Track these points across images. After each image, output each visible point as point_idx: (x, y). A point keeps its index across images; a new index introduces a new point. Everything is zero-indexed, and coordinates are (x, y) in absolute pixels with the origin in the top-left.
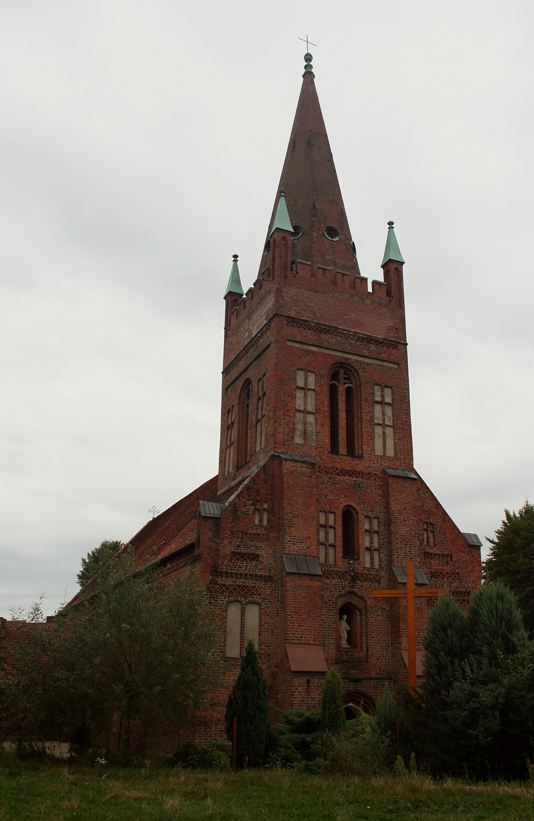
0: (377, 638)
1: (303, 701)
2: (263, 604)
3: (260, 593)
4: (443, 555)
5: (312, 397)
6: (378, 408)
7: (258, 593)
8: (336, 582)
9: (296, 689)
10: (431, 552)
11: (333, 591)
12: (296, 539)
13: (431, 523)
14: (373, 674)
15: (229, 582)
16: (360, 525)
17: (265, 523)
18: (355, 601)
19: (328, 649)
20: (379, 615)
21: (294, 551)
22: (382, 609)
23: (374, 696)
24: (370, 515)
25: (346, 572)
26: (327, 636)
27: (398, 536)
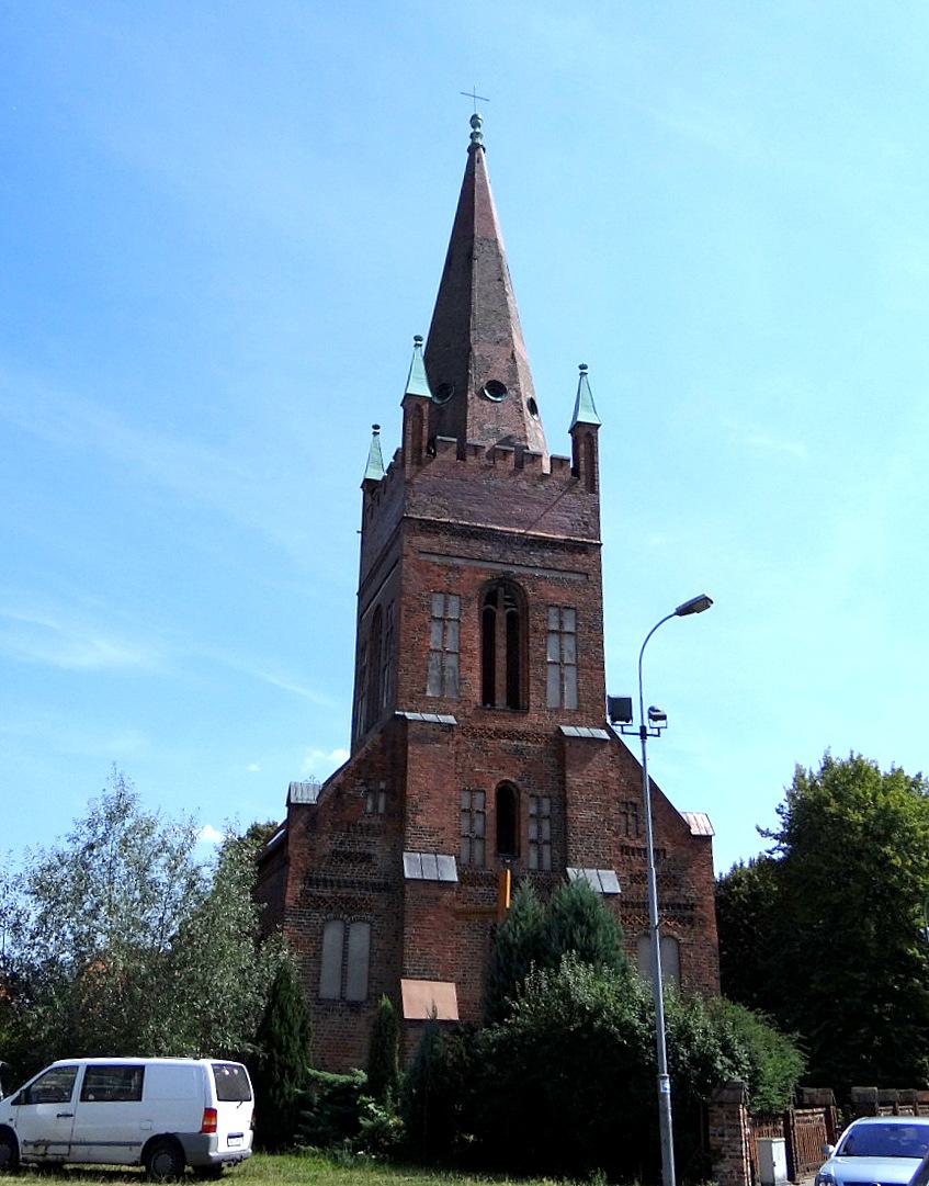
5: (454, 630)
6: (553, 640)
10: (632, 845)
13: (631, 803)
15: (327, 893)
16: (522, 810)
17: (381, 809)
24: (538, 793)
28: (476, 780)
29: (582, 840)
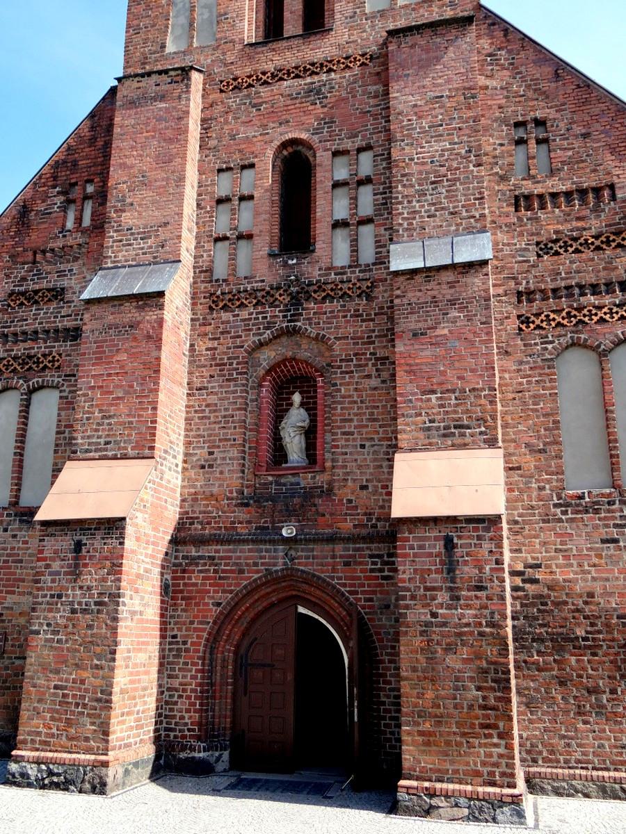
1: (60, 596)
2: (64, 388)
3: (59, 367)
4: (583, 192)
7: (57, 364)
8: (252, 314)
9: (48, 566)
10: (538, 190)
11: (240, 336)
12: (132, 234)
14: (347, 526)
17: (87, 222)
18: (305, 351)
19: (221, 473)
20: (369, 376)
21: (126, 261)
22: (377, 359)
23: (344, 585)
24: (348, 145)
25: (278, 288)
26: (220, 440)
27: (414, 169)
28: (240, 151)
29: (422, 194)
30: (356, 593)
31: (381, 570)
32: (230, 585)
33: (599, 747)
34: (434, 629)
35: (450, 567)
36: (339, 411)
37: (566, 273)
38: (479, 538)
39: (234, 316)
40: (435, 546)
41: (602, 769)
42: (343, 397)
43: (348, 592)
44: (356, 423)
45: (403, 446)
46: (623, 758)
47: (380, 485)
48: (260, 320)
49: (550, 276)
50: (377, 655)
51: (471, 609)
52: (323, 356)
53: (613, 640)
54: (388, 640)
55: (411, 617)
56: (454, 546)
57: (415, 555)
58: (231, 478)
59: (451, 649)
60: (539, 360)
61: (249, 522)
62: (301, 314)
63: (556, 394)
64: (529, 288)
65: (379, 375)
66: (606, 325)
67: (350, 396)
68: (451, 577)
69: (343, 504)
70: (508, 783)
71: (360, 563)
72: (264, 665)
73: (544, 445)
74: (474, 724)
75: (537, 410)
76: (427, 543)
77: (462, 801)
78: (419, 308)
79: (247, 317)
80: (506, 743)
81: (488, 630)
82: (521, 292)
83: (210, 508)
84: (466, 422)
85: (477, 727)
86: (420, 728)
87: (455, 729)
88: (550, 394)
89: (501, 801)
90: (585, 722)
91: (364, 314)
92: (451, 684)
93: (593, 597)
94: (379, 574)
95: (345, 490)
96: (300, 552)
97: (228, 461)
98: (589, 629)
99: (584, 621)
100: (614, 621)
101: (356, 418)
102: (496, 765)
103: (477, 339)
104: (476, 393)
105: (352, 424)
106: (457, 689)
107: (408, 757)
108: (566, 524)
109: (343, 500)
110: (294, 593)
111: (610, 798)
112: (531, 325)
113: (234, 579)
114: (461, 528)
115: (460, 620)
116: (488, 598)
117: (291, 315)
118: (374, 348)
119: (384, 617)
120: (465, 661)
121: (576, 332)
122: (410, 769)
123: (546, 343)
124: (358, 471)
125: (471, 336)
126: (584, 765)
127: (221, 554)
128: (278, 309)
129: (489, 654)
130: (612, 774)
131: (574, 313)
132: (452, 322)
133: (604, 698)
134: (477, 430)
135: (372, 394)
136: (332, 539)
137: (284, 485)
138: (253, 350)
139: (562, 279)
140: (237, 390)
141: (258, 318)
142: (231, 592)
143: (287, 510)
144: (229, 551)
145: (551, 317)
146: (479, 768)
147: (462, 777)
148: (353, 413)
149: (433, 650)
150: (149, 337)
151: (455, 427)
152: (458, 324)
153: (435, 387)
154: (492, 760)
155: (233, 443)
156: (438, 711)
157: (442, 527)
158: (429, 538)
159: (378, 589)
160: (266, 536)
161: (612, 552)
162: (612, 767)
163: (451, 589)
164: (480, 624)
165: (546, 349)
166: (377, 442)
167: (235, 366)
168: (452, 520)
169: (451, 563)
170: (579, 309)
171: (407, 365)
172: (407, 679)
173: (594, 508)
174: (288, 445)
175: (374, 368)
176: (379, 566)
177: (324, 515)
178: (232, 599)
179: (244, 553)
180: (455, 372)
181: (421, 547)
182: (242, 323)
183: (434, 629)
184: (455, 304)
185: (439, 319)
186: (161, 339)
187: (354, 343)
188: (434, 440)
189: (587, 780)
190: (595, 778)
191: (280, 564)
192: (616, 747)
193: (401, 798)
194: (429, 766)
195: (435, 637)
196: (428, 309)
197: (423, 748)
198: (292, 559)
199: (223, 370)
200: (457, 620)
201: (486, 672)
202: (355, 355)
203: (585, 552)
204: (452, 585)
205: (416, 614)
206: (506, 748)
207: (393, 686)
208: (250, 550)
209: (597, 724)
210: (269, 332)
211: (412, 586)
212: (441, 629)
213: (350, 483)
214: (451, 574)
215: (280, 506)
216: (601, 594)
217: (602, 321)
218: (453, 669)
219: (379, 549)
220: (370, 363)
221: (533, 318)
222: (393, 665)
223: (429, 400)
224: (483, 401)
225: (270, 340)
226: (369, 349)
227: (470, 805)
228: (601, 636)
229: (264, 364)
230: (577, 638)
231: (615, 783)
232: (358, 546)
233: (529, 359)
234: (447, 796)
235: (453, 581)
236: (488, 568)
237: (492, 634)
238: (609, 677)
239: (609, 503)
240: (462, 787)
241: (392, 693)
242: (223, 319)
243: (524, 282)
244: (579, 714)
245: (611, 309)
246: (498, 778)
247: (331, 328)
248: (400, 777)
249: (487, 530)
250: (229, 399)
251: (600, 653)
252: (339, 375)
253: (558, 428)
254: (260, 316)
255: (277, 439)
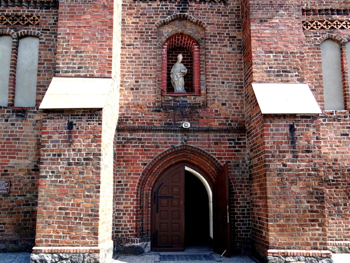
0: (221, 76)
1: (59, 155)
2: (42, 37)
3: (38, 24)
7: (36, 22)
8: (159, 5)
9: (50, 137)
11: (152, 17)
14: (215, 124)
18: (189, 30)
19: (144, 93)
20: (226, 46)
22: (230, 37)
23: (215, 154)
26: (142, 75)
30: (221, 158)
31: (234, 147)
32: (151, 154)
33: (338, 230)
34: (285, 172)
35: (293, 141)
36: (210, 63)
37: (326, 2)
38: (308, 126)
39: (148, 5)
40: (284, 130)
41: (339, 240)
42: (212, 56)
43: (218, 158)
44: (219, 70)
45: (255, 80)
46: (349, 234)
47: (232, 103)
48: (164, 9)
49: (318, 3)
50: (233, 190)
51: (304, 162)
52: (199, 33)
53: (346, 181)
54: (239, 182)
55: (272, 166)
56: (295, 130)
57: (274, 134)
58: (149, 96)
59: (293, 182)
60: (313, 45)
61: (161, 120)
62: (188, 9)
63: (321, 62)
64: (308, 8)
65: (231, 46)
66: (345, 30)
67: (216, 56)
68: (293, 146)
69: (213, 113)
70: (323, 248)
71: (223, 143)
72: (168, 197)
73: (315, 87)
74: (306, 220)
75: (311, 70)
76: (280, 128)
77: (302, 258)
78: (263, 7)
79: (156, 7)
80: (323, 228)
81: (313, 173)
82: (304, 9)
83: (137, 112)
84: (288, 69)
85: (308, 221)
86: (278, 223)
87: (296, 223)
88: (318, 62)
89: (321, 256)
90: (332, 219)
91: (223, 12)
92: (294, 200)
93: (337, 161)
94: (233, 149)
95: (214, 105)
96: (191, 137)
97: (147, 87)
98: (335, 176)
99: (333, 172)
100: (346, 172)
101: (219, 68)
102: (318, 239)
103: (294, 27)
104: (293, 55)
105: (217, 71)
106: (297, 202)
107: (272, 238)
108: (325, 126)
109: (212, 110)
110: (184, 159)
111: (344, 252)
112: (309, 27)
113: (153, 151)
114: (298, 120)
115: (298, 167)
116: (312, 156)
117: (182, 9)
118: (228, 31)
119: (236, 171)
120: (301, 188)
121: (331, 32)
122: (273, 244)
123: (316, 36)
124: (221, 96)
125: (290, 25)
126: (332, 239)
127: (145, 137)
128: (174, 4)
129: (314, 184)
130: (344, 242)
131: (329, 23)
132: (281, 16)
133: (341, 208)
134: (294, 74)
135: (228, 56)
136: (208, 131)
137: (178, 102)
138: (160, 26)
139: (324, 5)
140: (151, 47)
141: (163, 8)
142: (152, 158)
143: (182, 115)
144: (150, 136)
145: (318, 24)
146: (309, 241)
147: (300, 246)
148: (218, 65)
149: (284, 183)
150: (105, 7)
151: (283, 72)
152: (284, 18)
153: (272, 50)
154: (316, 237)
155: (150, 76)
156: (287, 214)
157: (288, 119)
158: (281, 126)
159: (233, 156)
160: (168, 128)
161: (346, 140)
162: (344, 239)
163: (293, 152)
164: (309, 170)
165: (316, 39)
166: (230, 81)
167: (149, 33)
168: (294, 116)
169: (293, 138)
170: (332, 21)
171: (257, 37)
172: (270, 198)
173: (337, 119)
174: (176, 82)
175: (229, 42)
176: (233, 145)
177: (202, 118)
178: (153, 161)
179: (159, 137)
180: (282, 43)
181: (277, 130)
182: (154, 10)
183: (285, 172)
184: (282, 7)
185: (274, 14)
186: (113, 8)
187: (217, 27)
188: (272, 78)
189: (334, 245)
190: (337, 244)
191: (180, 143)
192: (346, 230)
193: (270, 259)
194: (283, 242)
195: (285, 177)
196: (268, 8)
197: (280, 233)
198: (185, 141)
199: (143, 35)
200: (297, 168)
201: (312, 194)
202: (218, 34)
203: (334, 140)
204: (294, 150)
205: (275, 165)
206: (323, 231)
207: (241, 205)
208: (162, 136)
209: (338, 220)
210: (169, 16)
211: (272, 150)
212: (288, 172)
213: (216, 102)
214: (293, 144)
215: (178, 112)
216: (341, 160)
217: (342, 28)
218: (295, 193)
219: (233, 136)
220: (226, 39)
221: (309, 24)
222: (241, 195)
223: (269, 56)
224: (297, 59)
225: (170, 21)
226: (225, 31)
227: (306, 260)
228: (340, 179)
229: (166, 35)
230: (329, 180)
231: (346, 246)
232: (222, 134)
233: (308, 44)
234: (294, 256)
235: (294, 147)
236: (312, 141)
237: (315, 175)
238: (344, 198)
239: (345, 117)
240: (301, 251)
241: (241, 209)
242: (142, 6)
243: (305, 5)
244: (330, 215)
245: (346, 23)
246: (318, 246)
247: (204, 18)
248: (268, 248)
249: (312, 122)
250: (147, 52)
251: (340, 187)
252: (209, 44)
253: (321, 79)
254: (164, 7)
255: (169, 79)
